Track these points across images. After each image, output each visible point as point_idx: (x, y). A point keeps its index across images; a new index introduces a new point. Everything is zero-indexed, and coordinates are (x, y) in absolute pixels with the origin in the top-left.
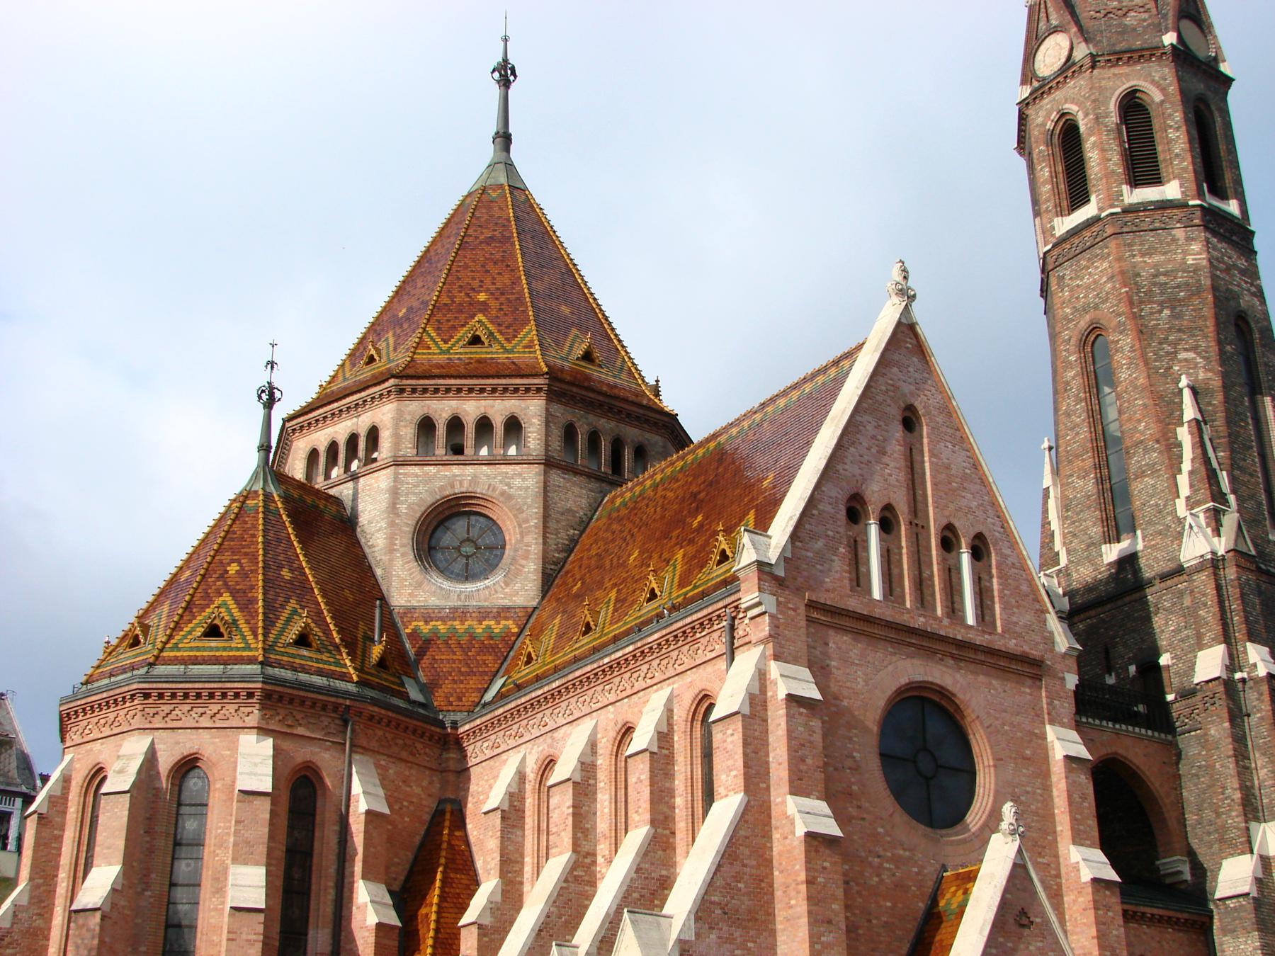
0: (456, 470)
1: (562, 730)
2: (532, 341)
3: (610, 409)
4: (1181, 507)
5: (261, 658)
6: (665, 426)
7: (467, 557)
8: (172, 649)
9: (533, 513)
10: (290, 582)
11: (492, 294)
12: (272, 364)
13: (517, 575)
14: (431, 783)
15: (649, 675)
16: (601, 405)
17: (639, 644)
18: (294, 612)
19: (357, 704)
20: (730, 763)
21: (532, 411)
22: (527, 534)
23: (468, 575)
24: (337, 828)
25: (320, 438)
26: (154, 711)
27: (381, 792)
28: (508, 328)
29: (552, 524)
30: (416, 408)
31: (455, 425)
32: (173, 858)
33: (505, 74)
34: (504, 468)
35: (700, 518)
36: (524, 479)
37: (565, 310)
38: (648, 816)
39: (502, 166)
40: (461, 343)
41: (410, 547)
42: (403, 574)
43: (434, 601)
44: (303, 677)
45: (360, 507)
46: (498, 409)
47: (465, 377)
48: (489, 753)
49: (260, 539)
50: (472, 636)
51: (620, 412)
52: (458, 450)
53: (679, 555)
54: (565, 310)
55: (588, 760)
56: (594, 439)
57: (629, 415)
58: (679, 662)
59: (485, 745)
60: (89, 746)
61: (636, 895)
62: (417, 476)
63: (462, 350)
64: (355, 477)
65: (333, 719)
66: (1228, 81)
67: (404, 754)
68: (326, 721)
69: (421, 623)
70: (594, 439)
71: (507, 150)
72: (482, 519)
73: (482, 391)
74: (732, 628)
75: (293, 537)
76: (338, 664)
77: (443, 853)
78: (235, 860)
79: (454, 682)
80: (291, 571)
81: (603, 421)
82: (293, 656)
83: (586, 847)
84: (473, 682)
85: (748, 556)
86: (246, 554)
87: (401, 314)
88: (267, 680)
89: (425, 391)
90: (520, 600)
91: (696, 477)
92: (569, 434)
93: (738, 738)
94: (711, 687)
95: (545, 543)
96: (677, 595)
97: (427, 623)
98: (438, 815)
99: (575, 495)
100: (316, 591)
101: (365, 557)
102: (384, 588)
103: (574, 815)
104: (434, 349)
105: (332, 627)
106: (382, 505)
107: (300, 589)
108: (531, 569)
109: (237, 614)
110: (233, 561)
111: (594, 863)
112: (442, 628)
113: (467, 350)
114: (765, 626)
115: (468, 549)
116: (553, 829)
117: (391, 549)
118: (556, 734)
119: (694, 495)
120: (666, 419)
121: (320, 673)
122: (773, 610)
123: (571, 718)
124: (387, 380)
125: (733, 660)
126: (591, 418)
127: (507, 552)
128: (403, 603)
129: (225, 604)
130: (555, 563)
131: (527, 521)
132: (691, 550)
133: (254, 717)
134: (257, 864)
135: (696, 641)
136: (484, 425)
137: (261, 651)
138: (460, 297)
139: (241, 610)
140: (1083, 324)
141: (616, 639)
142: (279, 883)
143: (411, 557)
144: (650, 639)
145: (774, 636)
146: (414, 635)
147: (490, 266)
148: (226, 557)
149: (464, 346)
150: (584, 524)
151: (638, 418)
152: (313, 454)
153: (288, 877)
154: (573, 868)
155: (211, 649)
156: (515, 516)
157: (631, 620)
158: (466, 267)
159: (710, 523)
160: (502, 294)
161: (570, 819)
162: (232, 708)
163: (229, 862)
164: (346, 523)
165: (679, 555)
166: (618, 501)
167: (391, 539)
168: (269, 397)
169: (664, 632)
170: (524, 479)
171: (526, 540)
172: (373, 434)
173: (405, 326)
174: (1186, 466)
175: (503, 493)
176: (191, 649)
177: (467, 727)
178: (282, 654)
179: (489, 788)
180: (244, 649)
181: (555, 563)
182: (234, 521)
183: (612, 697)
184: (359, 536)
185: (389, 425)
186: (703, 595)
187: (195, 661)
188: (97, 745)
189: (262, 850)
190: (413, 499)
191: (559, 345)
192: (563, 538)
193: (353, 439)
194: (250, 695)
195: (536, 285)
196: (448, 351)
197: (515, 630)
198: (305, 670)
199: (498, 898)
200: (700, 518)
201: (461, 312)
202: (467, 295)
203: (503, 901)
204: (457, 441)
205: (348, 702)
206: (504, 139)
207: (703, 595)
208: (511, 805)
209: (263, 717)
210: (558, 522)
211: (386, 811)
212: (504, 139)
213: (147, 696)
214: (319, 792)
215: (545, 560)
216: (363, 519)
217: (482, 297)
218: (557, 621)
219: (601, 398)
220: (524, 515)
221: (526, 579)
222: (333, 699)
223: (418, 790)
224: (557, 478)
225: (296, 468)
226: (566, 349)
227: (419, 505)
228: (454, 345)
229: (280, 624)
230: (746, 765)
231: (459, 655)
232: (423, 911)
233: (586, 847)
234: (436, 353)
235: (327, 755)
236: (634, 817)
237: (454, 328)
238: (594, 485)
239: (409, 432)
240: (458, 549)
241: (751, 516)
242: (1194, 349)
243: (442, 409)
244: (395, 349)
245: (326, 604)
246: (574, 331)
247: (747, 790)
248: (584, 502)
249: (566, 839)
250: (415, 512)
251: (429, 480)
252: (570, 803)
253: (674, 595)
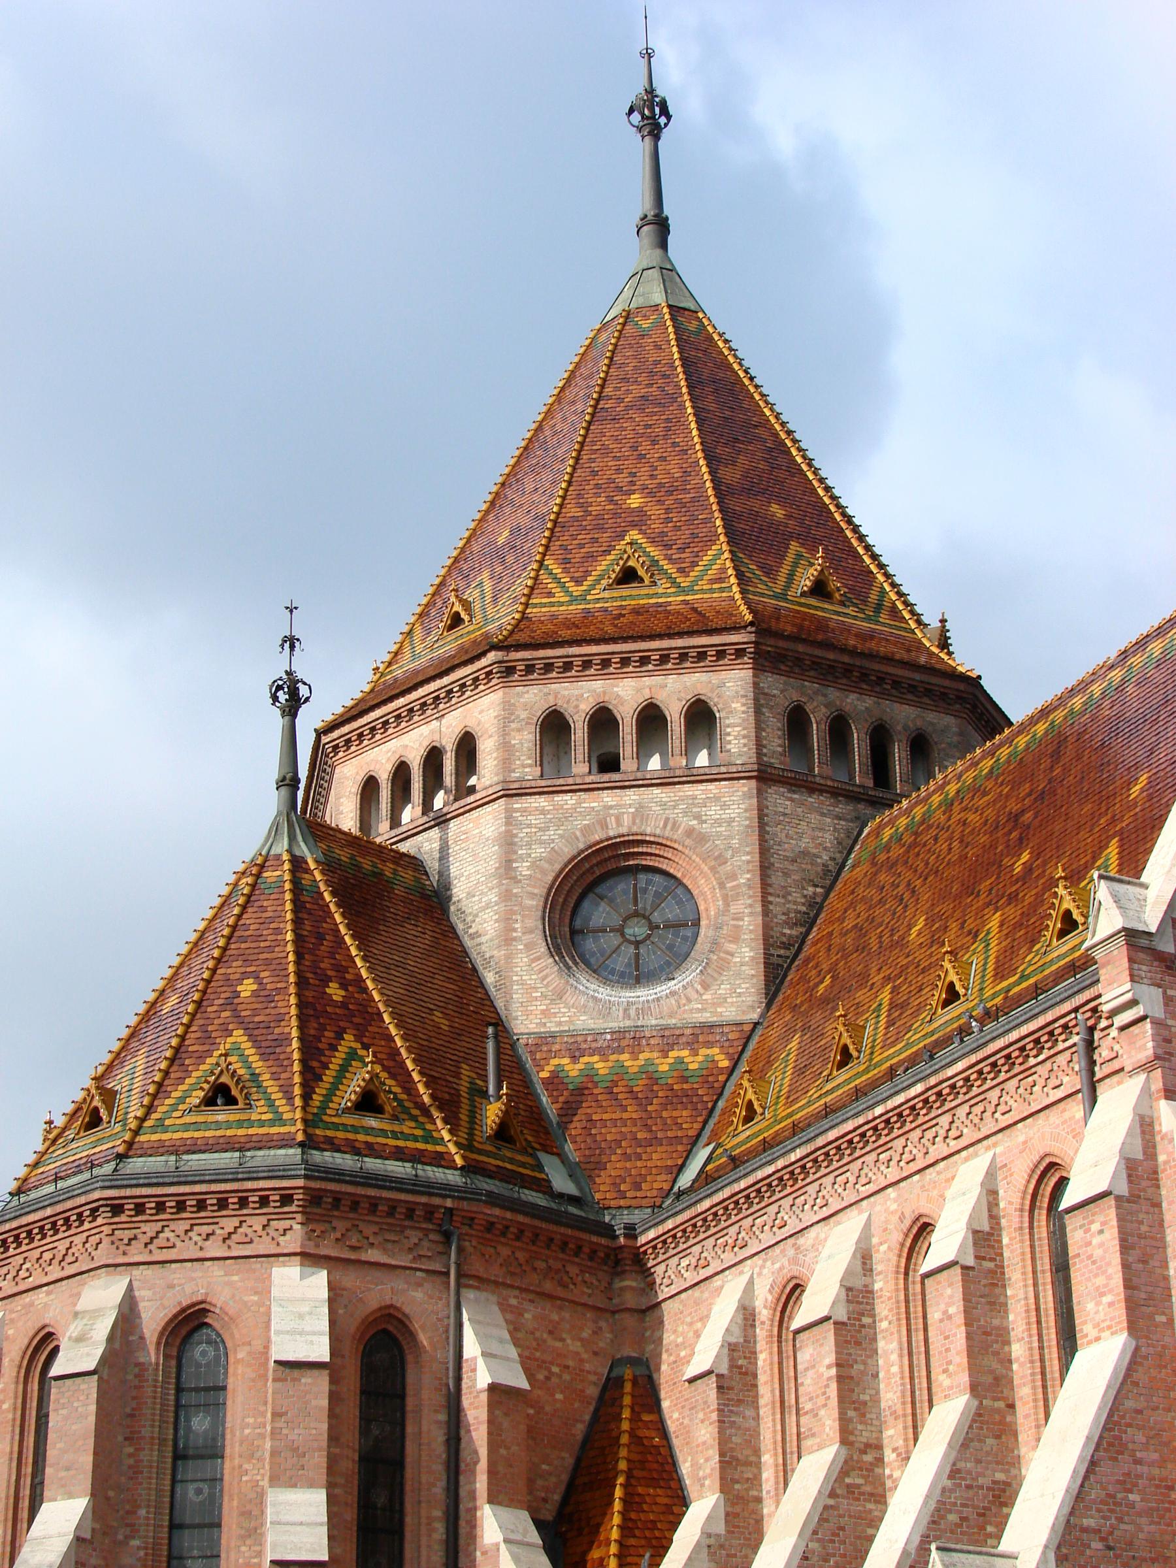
0: (608, 798)
1: (812, 1233)
2: (723, 570)
3: (864, 676)
5: (300, 1137)
6: (960, 698)
7: (637, 944)
8: (154, 1129)
9: (743, 862)
10: (344, 1005)
11: (651, 494)
12: (291, 642)
13: (720, 970)
14: (597, 1332)
15: (953, 1133)
16: (848, 670)
17: (933, 1081)
18: (352, 1055)
19: (465, 1205)
20: (1100, 1281)
21: (731, 689)
22: (736, 897)
23: (639, 976)
24: (442, 1417)
25: (379, 759)
26: (128, 1234)
27: (513, 1352)
28: (682, 550)
29: (777, 880)
30: (535, 698)
31: (603, 721)
32: (174, 1481)
33: (652, 115)
35: (1025, 857)
36: (724, 806)
37: (777, 511)
38: (964, 1378)
39: (654, 273)
40: (604, 582)
41: (539, 933)
42: (531, 979)
43: (585, 1022)
44: (372, 1164)
45: (454, 871)
46: (673, 690)
47: (614, 640)
48: (691, 1277)
49: (289, 936)
50: (653, 1079)
51: (881, 680)
52: (609, 763)
53: (994, 923)
54: (777, 511)
55: (858, 1283)
56: (839, 729)
57: (896, 684)
58: (1002, 1108)
59: (684, 1263)
60: (27, 1298)
61: (952, 1518)
62: (543, 812)
63: (606, 594)
64: (441, 821)
65: (426, 1232)
67: (548, 1286)
68: (414, 1236)
69: (566, 1061)
70: (839, 729)
71: (663, 244)
72: (657, 878)
73: (644, 661)
74: (1090, 1046)
75: (343, 929)
76: (429, 1138)
77: (623, 1452)
78: (275, 1480)
79: (626, 1157)
80: (343, 986)
81: (853, 697)
82: (355, 1129)
83: (864, 1435)
84: (658, 1157)
85: (1107, 920)
86: (267, 962)
87: (501, 540)
88: (313, 1172)
89: (548, 668)
91: (1015, 785)
92: (797, 723)
93: (1111, 1237)
94: (1059, 1149)
95: (766, 912)
96: (994, 994)
97: (574, 1059)
98: (612, 1385)
99: (812, 828)
100: (386, 1017)
101: (465, 953)
102: (500, 1004)
103: (840, 1379)
104: (560, 596)
105: (416, 1076)
106: (488, 867)
107: (361, 1018)
108: (746, 956)
109: (258, 1065)
110: (245, 975)
111: (880, 1460)
112: (601, 1067)
113: (615, 594)
114: (1144, 1043)
115: (637, 930)
116: (806, 1406)
117: (507, 939)
118: (801, 1241)
119: (1015, 818)
120: (962, 687)
121: (399, 1155)
122: (1159, 1012)
123: (826, 1212)
124: (484, 654)
125: (1094, 1100)
126: (833, 694)
127: (703, 931)
128: (532, 1028)
129: (237, 1048)
130: (786, 946)
131: (733, 877)
132: (1013, 912)
133: (295, 1236)
134: (311, 1485)
135: (1028, 1071)
136: (651, 719)
137: (299, 1125)
138: (599, 504)
139: (264, 1056)
141: (891, 1073)
142: (350, 1515)
143: (543, 949)
144: (950, 1072)
145: (1161, 1058)
146: (555, 1082)
147: (645, 446)
148: (235, 968)
149: (609, 587)
150: (832, 876)
151: (912, 688)
152: (370, 786)
153: (365, 1505)
154: (844, 1472)
155: (218, 1125)
156: (712, 869)
157: (917, 1038)
158: (606, 451)
159: (1044, 863)
160: (670, 493)
161: (834, 1386)
162: (257, 1223)
163: (265, 1483)
164: (432, 902)
165: (994, 923)
166: (887, 833)
167: (507, 921)
168: (290, 696)
169: (973, 1058)
170: (724, 806)
171: (733, 909)
172: (467, 746)
173: (510, 559)
175: (690, 832)
176: (186, 1127)
177: (651, 1234)
178: (336, 1127)
179: (696, 1336)
180: (272, 1123)
181: (786, 946)
182: (244, 908)
183: (893, 1174)
184: (454, 919)
185: (492, 730)
186: (1037, 990)
187: (194, 1148)
188: (41, 1296)
189: (319, 1460)
190: (539, 851)
191: (770, 572)
192: (797, 901)
193: (433, 757)
194: (286, 1199)
195: (727, 474)
196: (583, 598)
197: (725, 1064)
198: (372, 1150)
199: (720, 1528)
201: (601, 528)
202: (610, 500)
203: (728, 1532)
204: (608, 748)
205: (449, 1203)
206: (659, 226)
207: (1037, 990)
208: (733, 1365)
209: (309, 1235)
210: (786, 874)
211: (524, 1384)
213: (117, 1210)
214: (410, 1358)
215: (768, 941)
216: (459, 891)
217: (635, 501)
218: (794, 1044)
219: (846, 659)
220: (728, 867)
221: (738, 975)
222: (423, 1199)
223: (574, 1346)
224: (780, 800)
225: (343, 813)
226: (782, 579)
227: (550, 861)
228: (593, 587)
229: (329, 1077)
230: (1128, 1285)
231: (632, 1112)
232: (595, 1554)
233: (864, 1435)
234: (562, 601)
235: (418, 1295)
236: (941, 1380)
237: (591, 557)
238: (843, 808)
239: (526, 739)
240: (621, 931)
241: (1112, 851)
243: (578, 697)
244: (495, 599)
245: (404, 1038)
246: (794, 546)
247: (1132, 1328)
248: (828, 838)
249: (828, 1421)
250: (544, 872)
251: (566, 816)
252: (831, 1358)
253: (988, 993)
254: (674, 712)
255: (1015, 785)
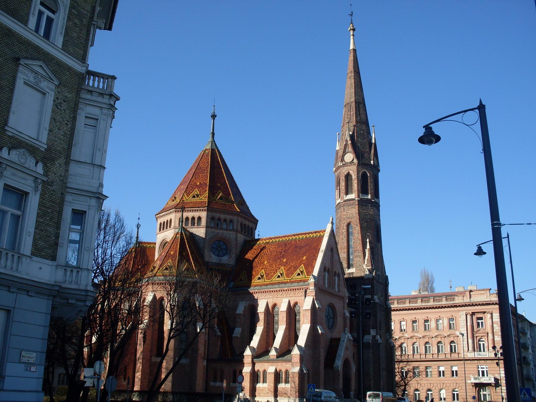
4: (365, 267)
33: (214, 116)
34: (229, 232)
35: (285, 260)
66: (379, 171)
90: (231, 263)
91: (279, 247)
132: (287, 268)
136: (225, 220)
140: (348, 221)
172: (199, 218)
174: (366, 258)
193: (193, 218)
200: (285, 260)
206: (213, 134)
212: (213, 134)
217: (219, 185)
242: (370, 233)
254: (228, 221)
255: (279, 247)
